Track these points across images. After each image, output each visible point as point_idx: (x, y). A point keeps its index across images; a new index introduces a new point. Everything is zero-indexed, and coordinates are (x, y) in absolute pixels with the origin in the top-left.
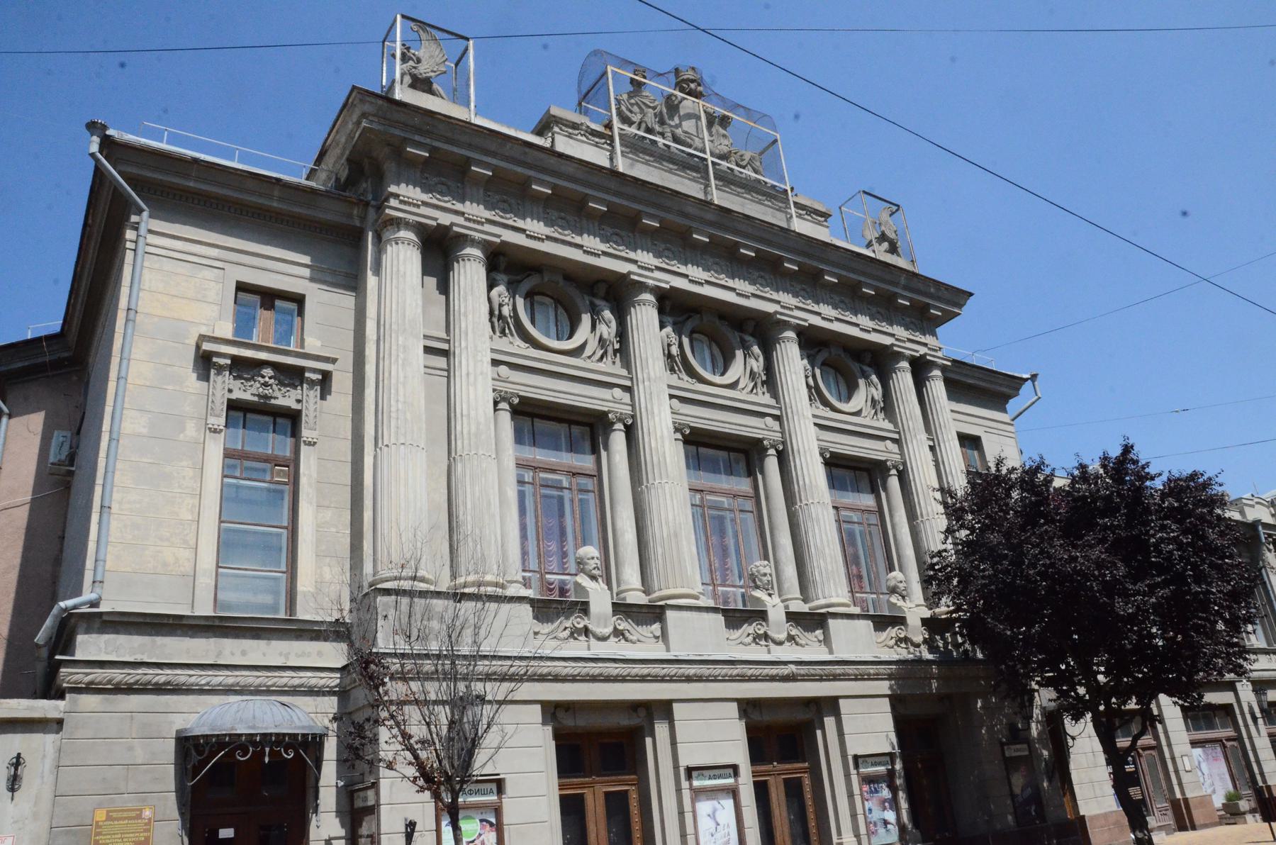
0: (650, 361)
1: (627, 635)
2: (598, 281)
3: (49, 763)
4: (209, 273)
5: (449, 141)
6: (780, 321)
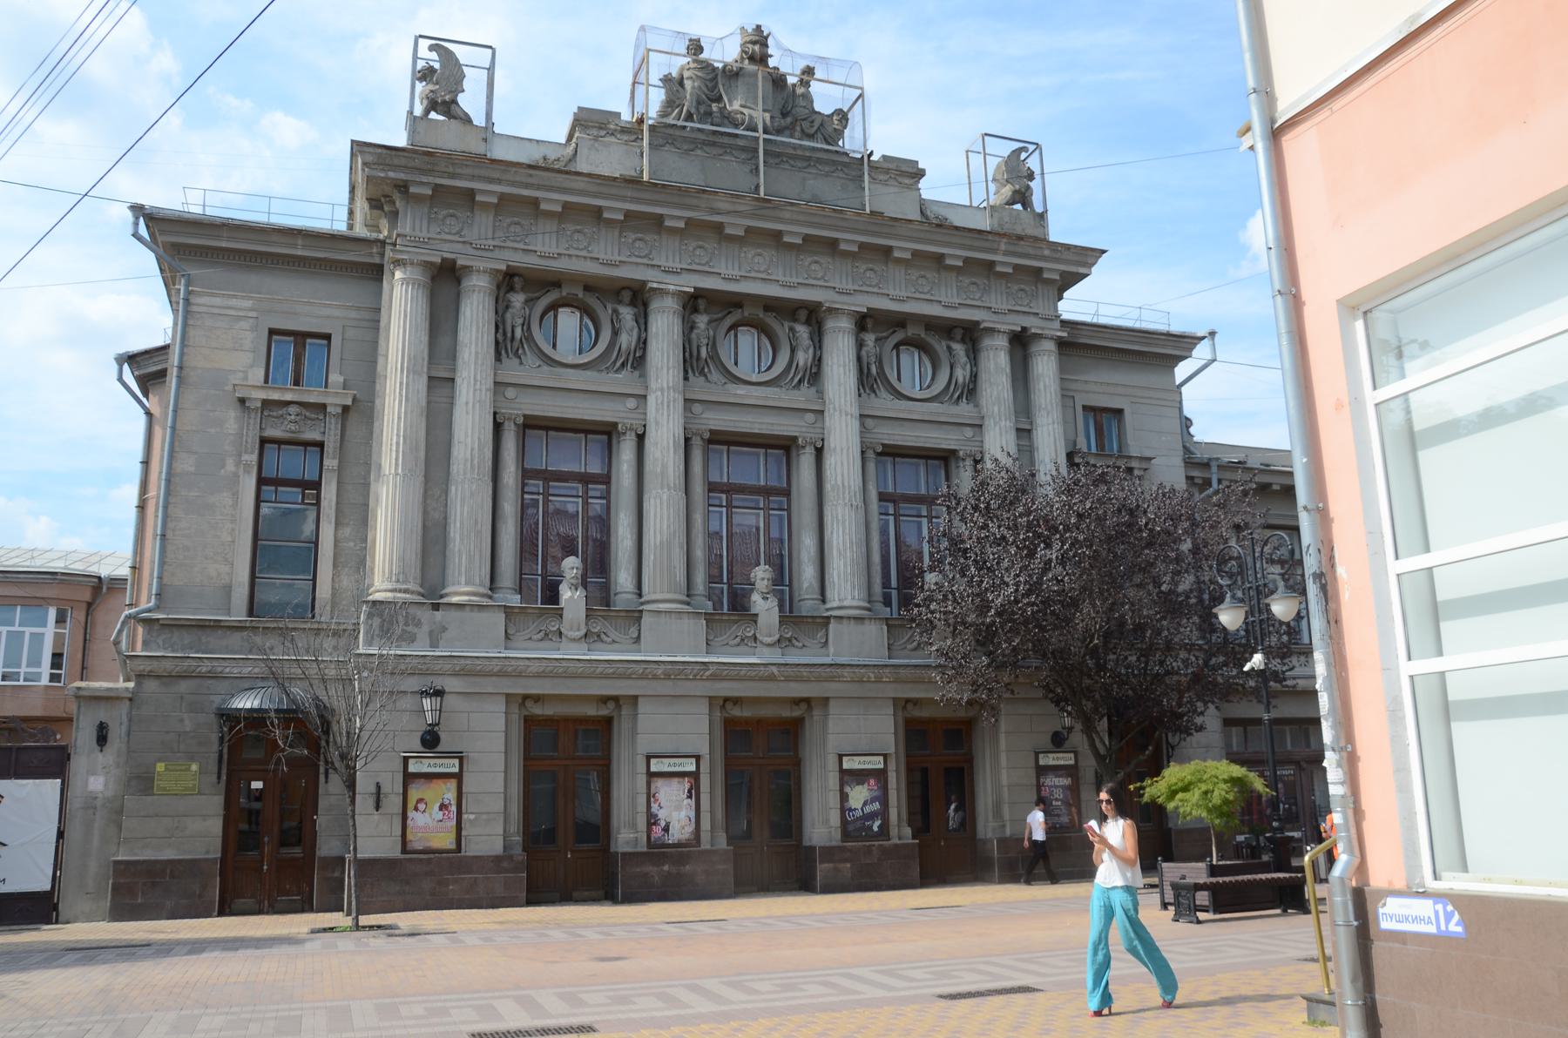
3: (124, 728)
4: (245, 324)
5: (453, 176)
6: (830, 310)
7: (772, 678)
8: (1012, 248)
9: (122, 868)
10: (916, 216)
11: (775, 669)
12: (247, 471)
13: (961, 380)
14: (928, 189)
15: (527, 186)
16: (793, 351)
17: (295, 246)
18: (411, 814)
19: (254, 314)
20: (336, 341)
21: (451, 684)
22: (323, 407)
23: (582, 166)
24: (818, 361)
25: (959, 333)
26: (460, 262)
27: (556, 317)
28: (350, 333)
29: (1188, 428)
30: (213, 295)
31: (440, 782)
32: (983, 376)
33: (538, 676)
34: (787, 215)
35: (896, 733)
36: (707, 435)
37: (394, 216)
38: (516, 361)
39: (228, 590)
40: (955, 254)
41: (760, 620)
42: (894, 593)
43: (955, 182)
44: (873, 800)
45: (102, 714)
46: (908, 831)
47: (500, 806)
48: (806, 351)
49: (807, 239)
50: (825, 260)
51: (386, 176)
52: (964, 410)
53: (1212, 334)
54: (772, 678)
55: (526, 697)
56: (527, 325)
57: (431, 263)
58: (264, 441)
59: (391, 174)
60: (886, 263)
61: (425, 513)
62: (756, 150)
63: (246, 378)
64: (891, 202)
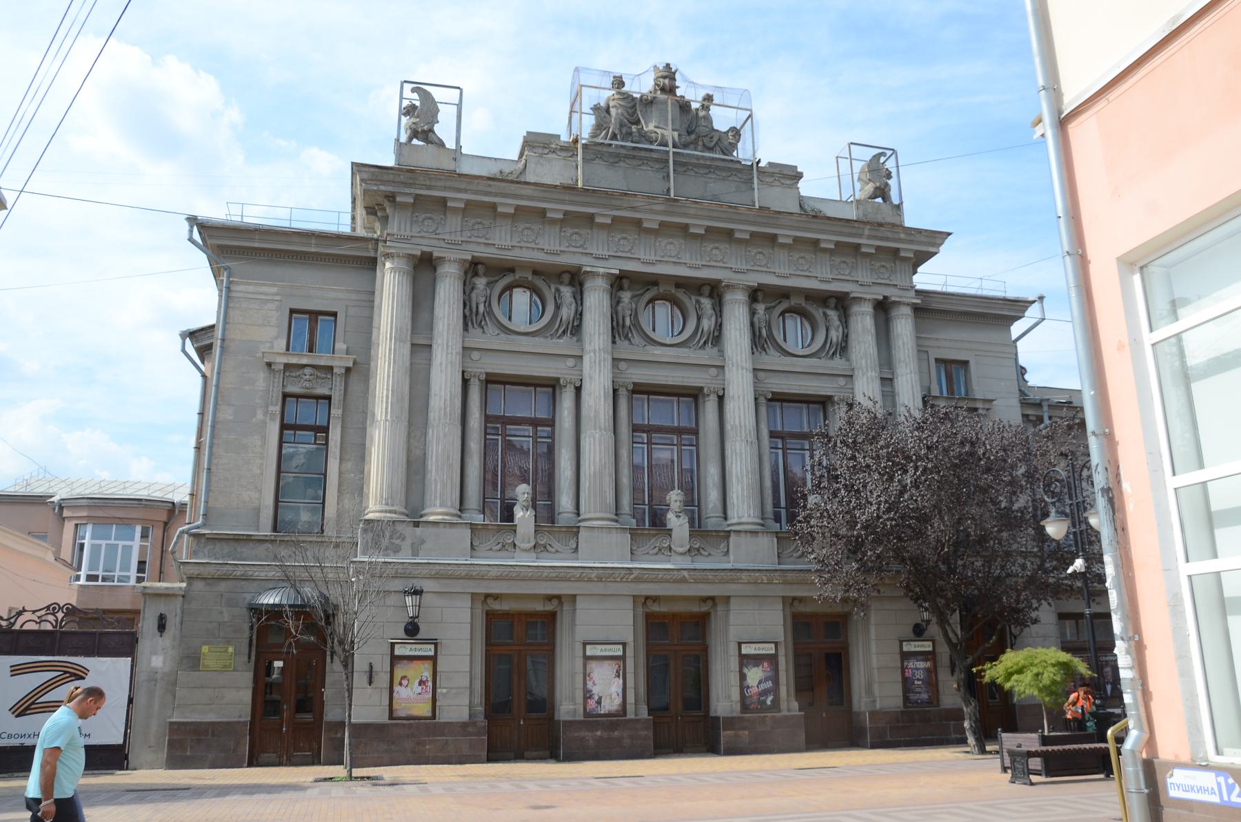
3: (178, 619)
4: (271, 306)
5: (429, 188)
7: (683, 581)
8: (874, 233)
10: (797, 210)
11: (686, 574)
12: (272, 419)
13: (835, 339)
14: (806, 188)
15: (487, 194)
16: (699, 319)
17: (310, 245)
18: (397, 688)
19: (278, 298)
20: (341, 318)
21: (428, 585)
22: (331, 368)
23: (530, 178)
24: (719, 327)
25: (832, 302)
27: (511, 296)
29: (1023, 375)
30: (248, 284)
31: (419, 662)
32: (852, 336)
33: (497, 579)
34: (692, 212)
35: (785, 625)
36: (631, 387)
37: (385, 220)
39: (257, 511)
40: (828, 239)
41: (674, 534)
42: (783, 512)
43: (827, 182)
44: (766, 679)
45: (162, 608)
46: (795, 705)
47: (466, 683)
48: (709, 319)
49: (709, 230)
50: (723, 246)
51: (379, 189)
52: (838, 364)
53: (1041, 298)
54: (683, 581)
55: (487, 596)
56: (488, 303)
57: (414, 256)
58: (285, 396)
59: (382, 188)
61: (409, 451)
62: (667, 161)
63: (272, 347)
64: (775, 198)
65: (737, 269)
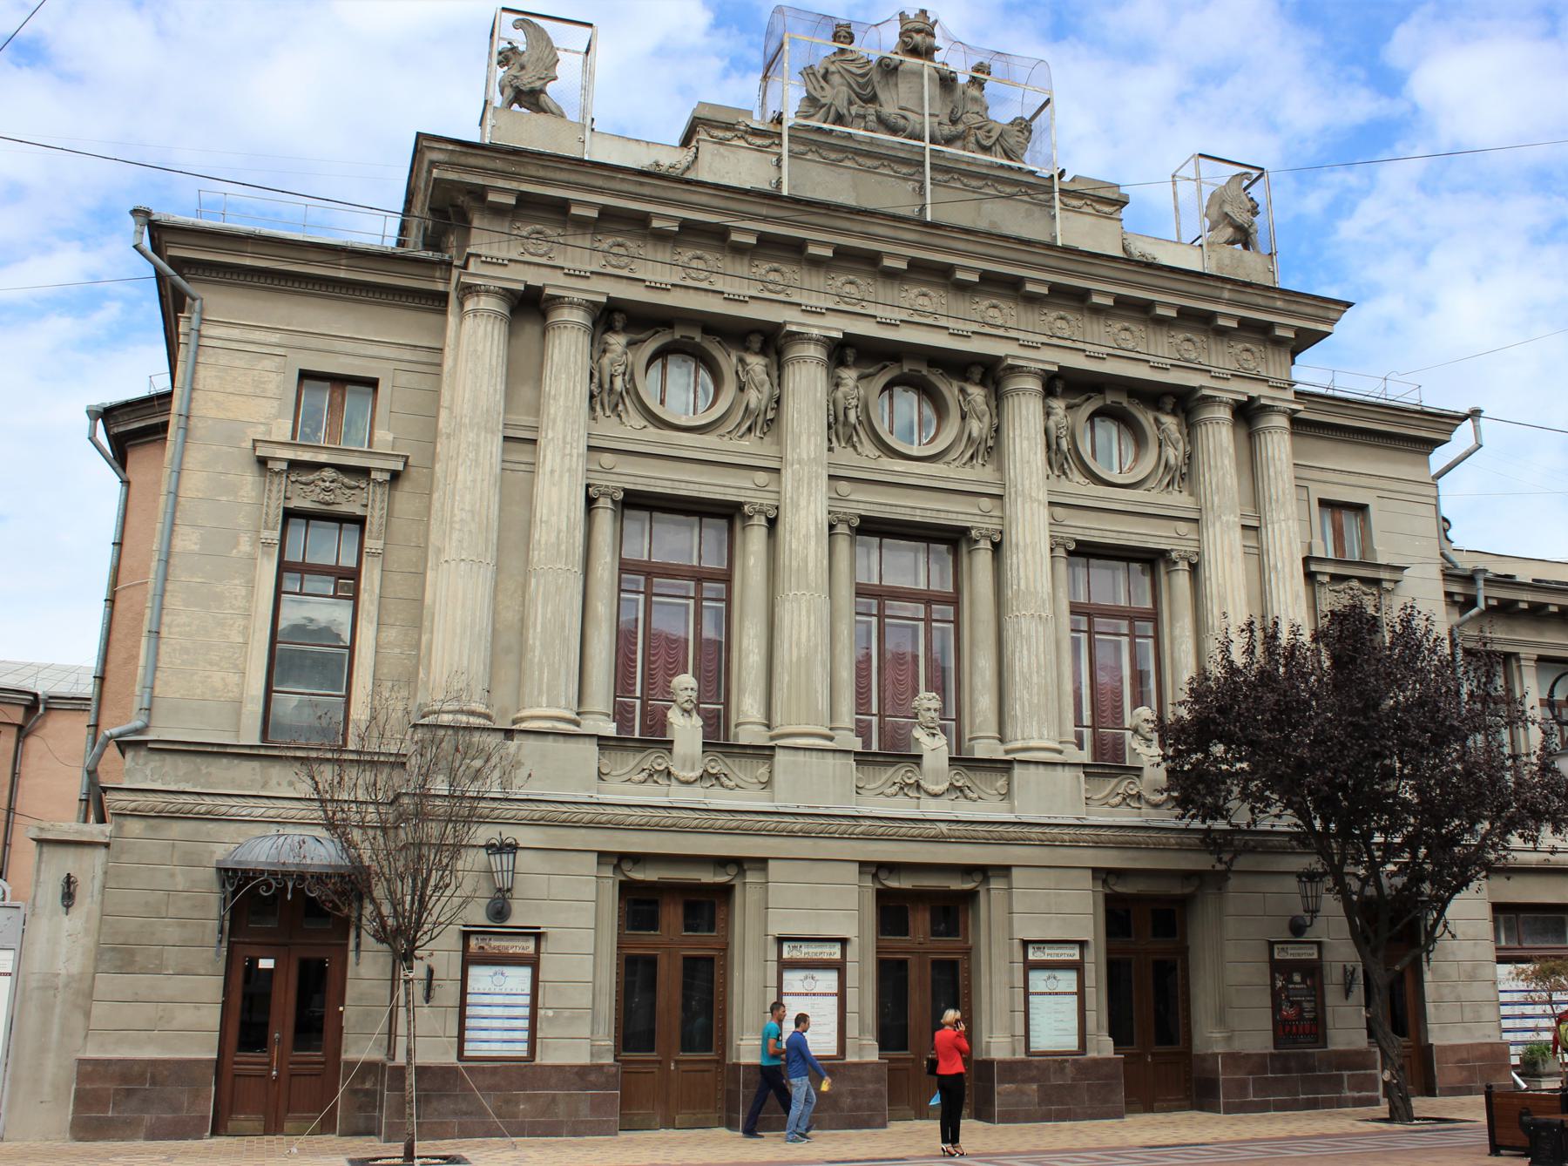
0: (804, 438)
1: (723, 779)
2: (752, 332)
4: (269, 363)
6: (1013, 368)
9: (89, 1071)
26: (548, 291)
28: (403, 379)
29: (1445, 531)
38: (614, 419)
39: (238, 703)
40: (1167, 303)
45: (67, 862)
47: (586, 1001)
58: (289, 514)
60: (1080, 310)
61: (495, 613)
62: (922, 164)
65: (1032, 340)
